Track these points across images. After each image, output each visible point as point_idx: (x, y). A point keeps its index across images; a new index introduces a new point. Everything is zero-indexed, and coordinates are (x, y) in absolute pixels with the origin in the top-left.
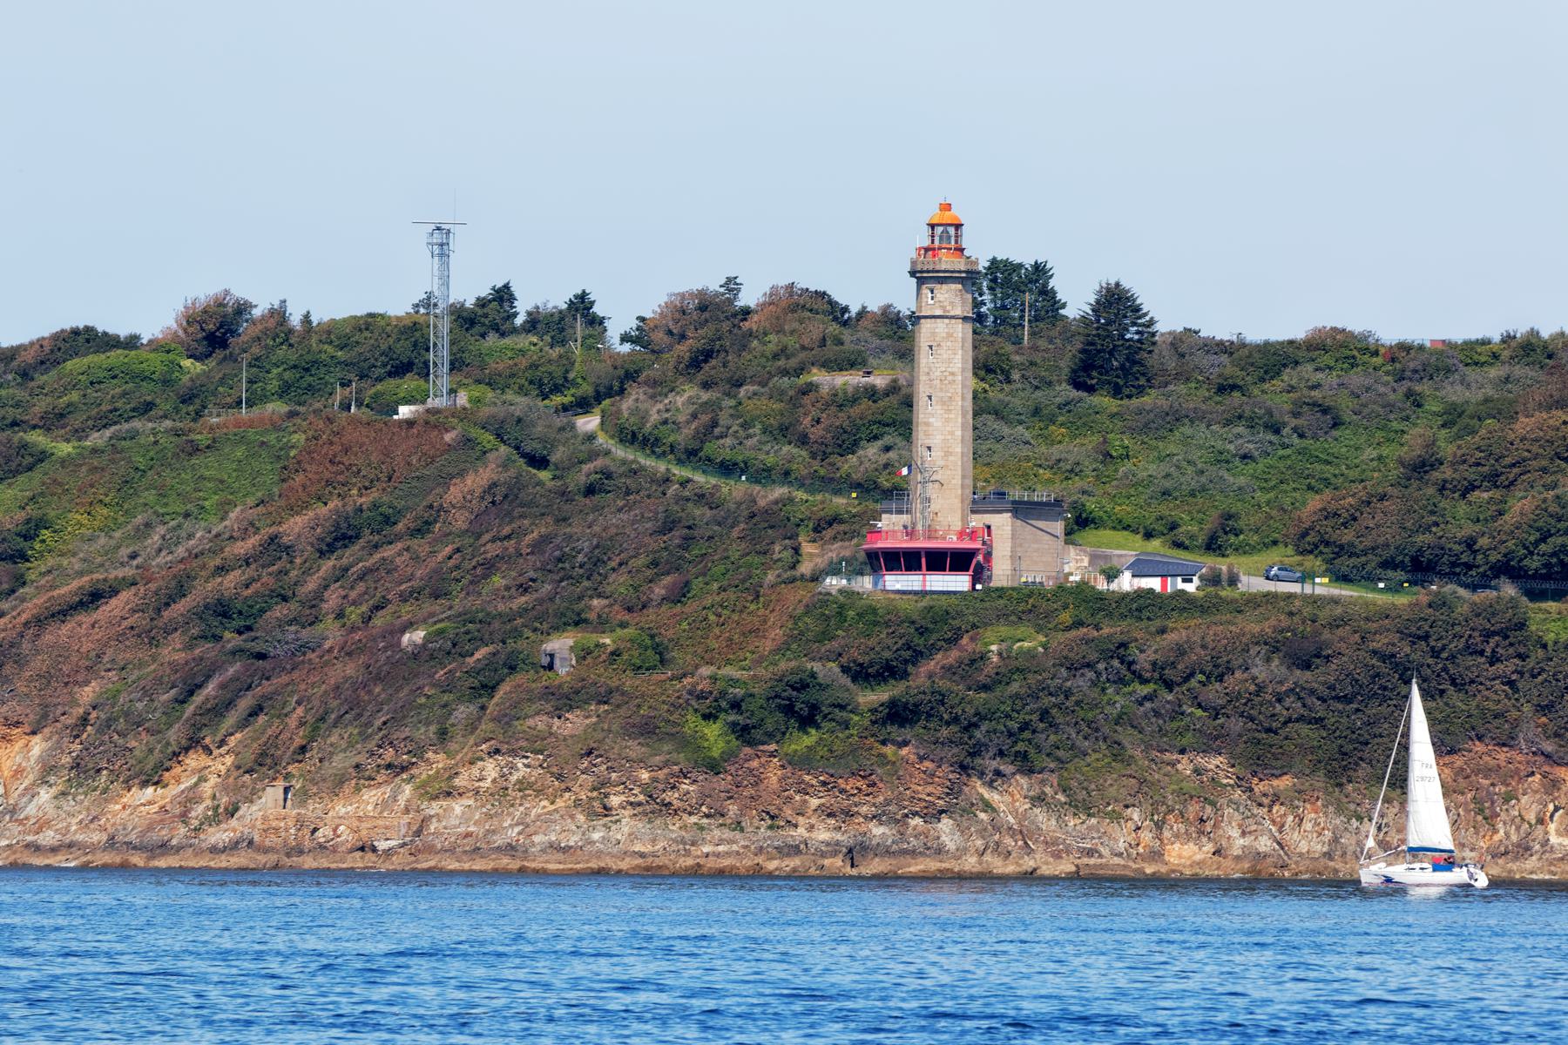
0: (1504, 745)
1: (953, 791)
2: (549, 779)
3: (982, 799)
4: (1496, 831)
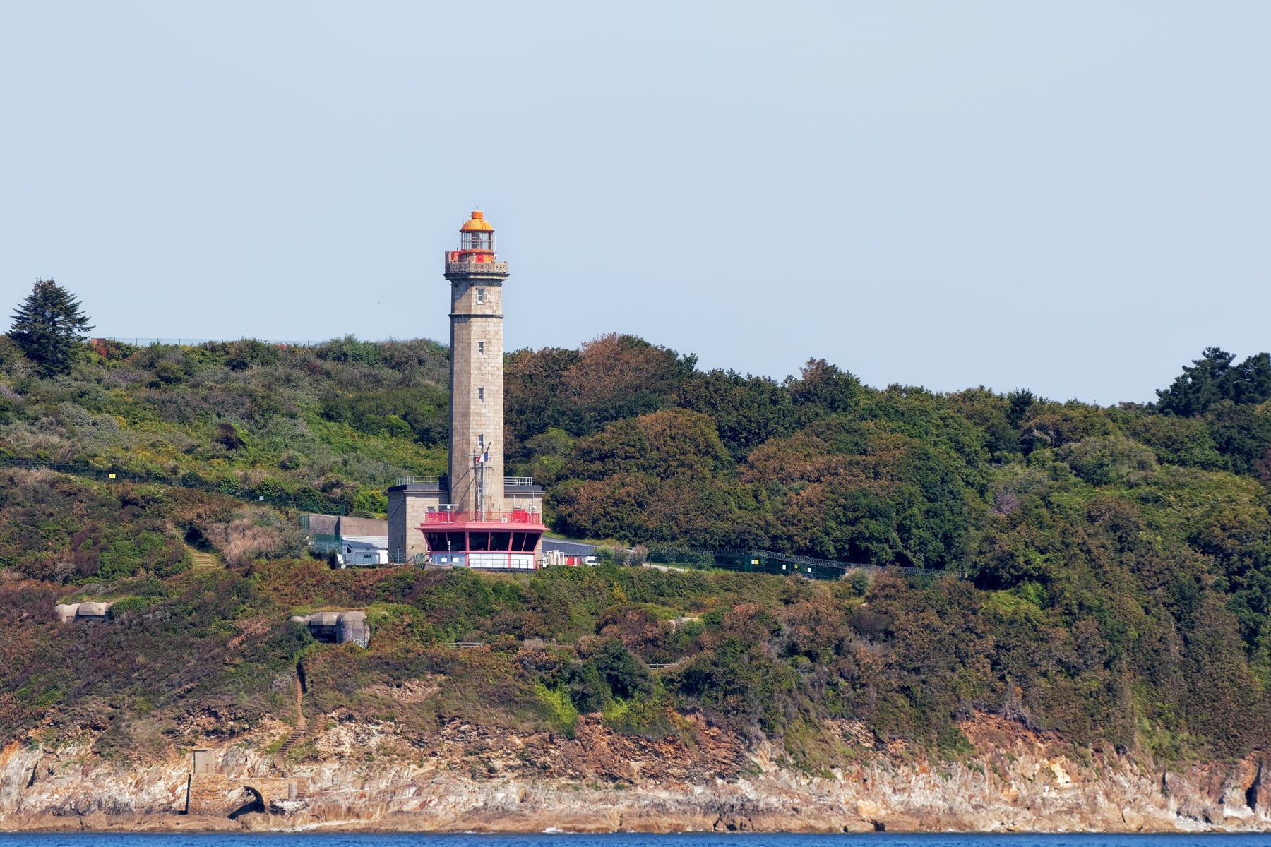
0: (993, 712)
2: (407, 746)
4: (1010, 785)
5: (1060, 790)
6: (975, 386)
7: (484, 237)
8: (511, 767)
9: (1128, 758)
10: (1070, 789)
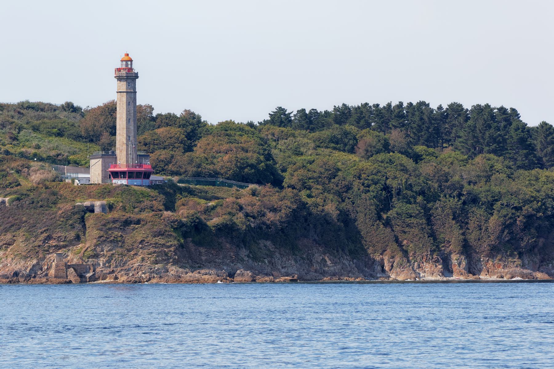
5: (329, 267)
6: (229, 120)
7: (129, 63)
8: (163, 259)
10: (332, 266)
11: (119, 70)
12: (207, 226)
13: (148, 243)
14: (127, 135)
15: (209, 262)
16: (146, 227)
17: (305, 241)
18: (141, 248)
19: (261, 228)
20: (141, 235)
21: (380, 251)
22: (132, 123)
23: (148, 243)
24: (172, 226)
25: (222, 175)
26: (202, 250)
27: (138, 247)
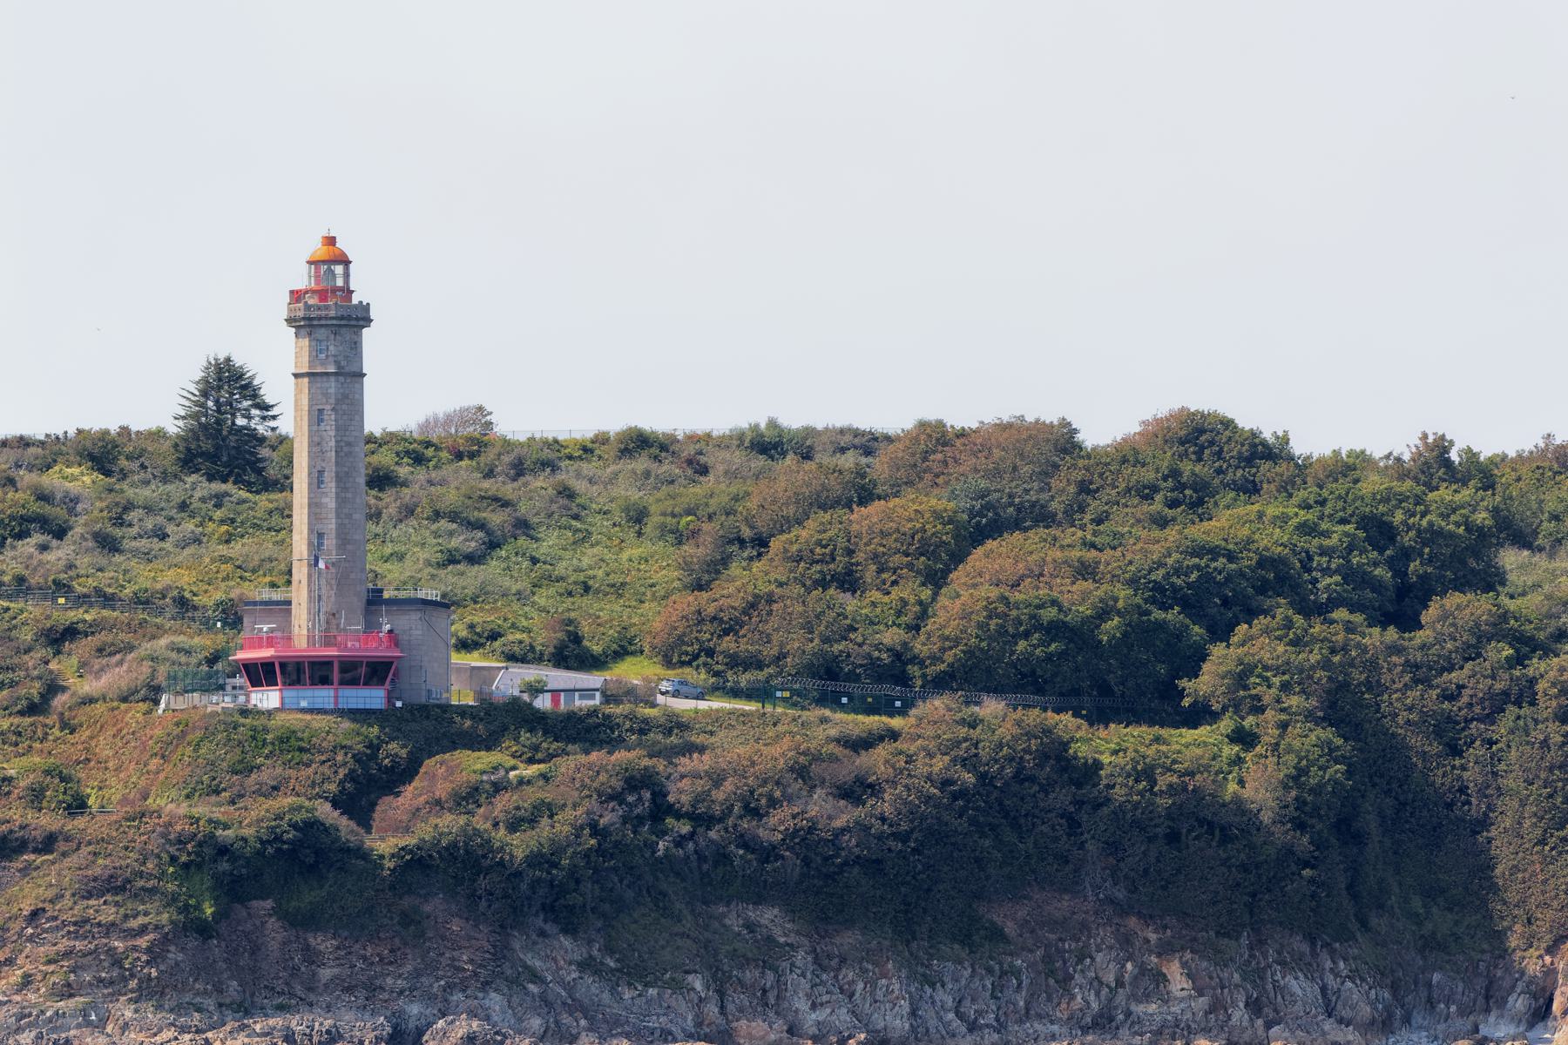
1: (501, 953)
3: (526, 967)
4: (1073, 997)
8: (101, 980)
9: (1332, 953)
10: (1182, 1000)
11: (296, 296)
12: (362, 854)
13: (55, 918)
14: (311, 530)
15: (349, 990)
16: (67, 862)
17: (1061, 906)
18: (31, 939)
19: (723, 857)
20: (41, 891)
21: (1548, 939)
22: (331, 486)
23: (55, 918)
24: (173, 859)
25: (922, 663)
26: (324, 943)
27: (20, 935)
